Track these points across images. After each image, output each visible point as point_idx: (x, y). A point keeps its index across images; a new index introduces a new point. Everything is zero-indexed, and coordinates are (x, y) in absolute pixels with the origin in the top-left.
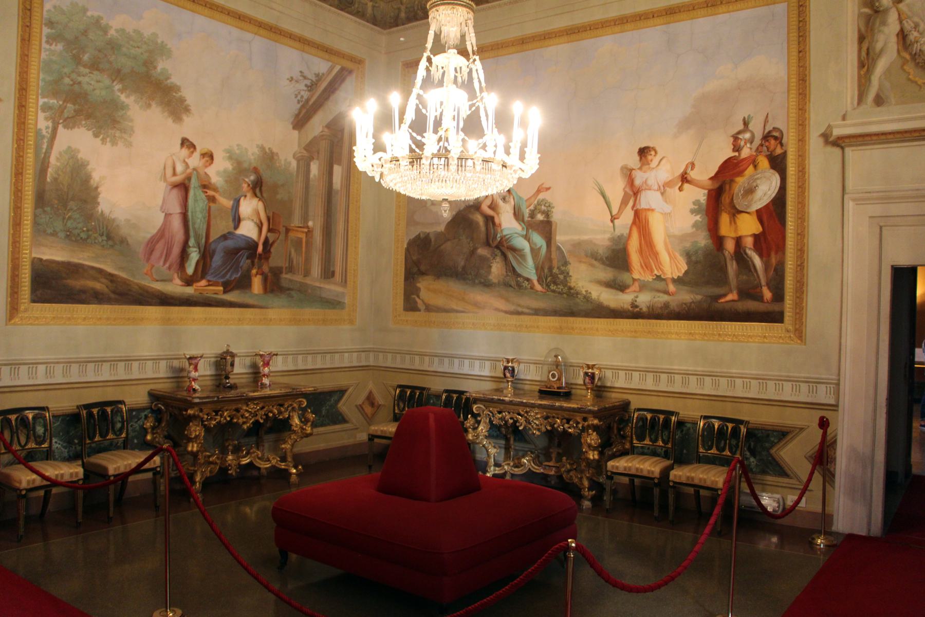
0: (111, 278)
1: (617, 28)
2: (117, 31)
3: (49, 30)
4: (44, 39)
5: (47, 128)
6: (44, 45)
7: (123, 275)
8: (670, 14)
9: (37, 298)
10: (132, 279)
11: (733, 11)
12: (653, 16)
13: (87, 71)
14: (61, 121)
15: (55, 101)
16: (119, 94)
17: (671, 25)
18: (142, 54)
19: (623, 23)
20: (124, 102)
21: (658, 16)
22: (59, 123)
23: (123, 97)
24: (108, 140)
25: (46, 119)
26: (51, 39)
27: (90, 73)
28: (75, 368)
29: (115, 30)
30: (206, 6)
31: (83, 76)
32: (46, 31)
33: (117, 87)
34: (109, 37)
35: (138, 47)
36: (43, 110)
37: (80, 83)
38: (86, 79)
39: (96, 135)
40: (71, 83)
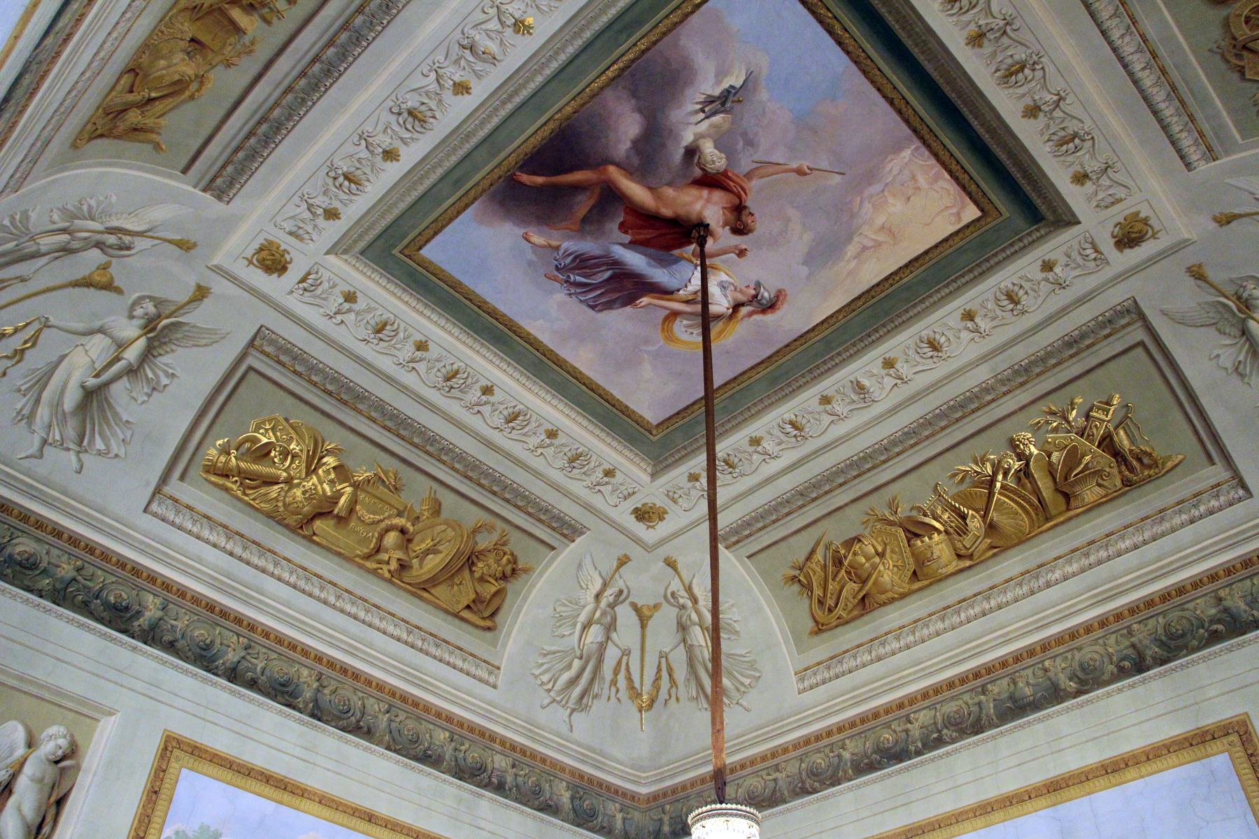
1: (980, 821)
8: (1055, 790)
11: (1149, 775)
12: (1030, 798)
17: (1059, 807)
19: (987, 813)
21: (1036, 797)
30: (386, 827)
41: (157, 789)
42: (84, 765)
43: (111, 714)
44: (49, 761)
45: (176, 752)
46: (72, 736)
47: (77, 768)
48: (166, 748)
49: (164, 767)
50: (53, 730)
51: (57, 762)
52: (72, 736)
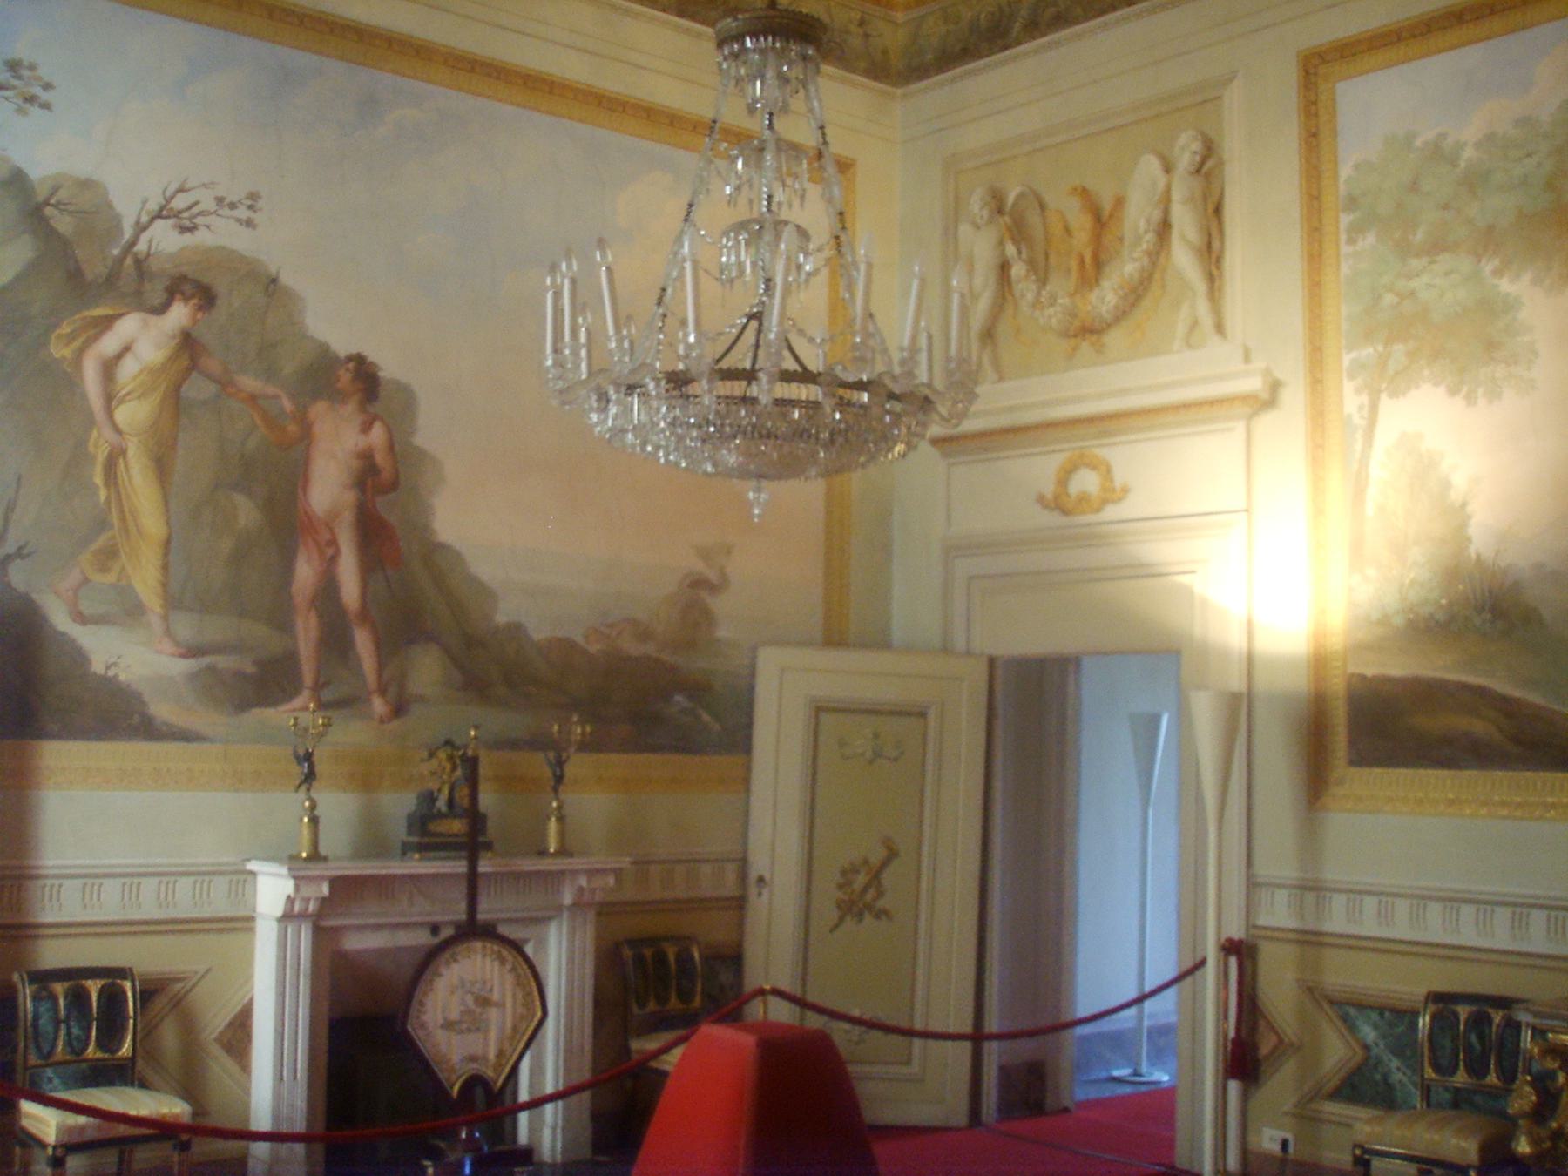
0: (1507, 707)
2: (1477, 145)
3: (1351, 217)
4: (1343, 237)
5: (1360, 408)
6: (1345, 249)
7: (1535, 698)
9: (1361, 759)
10: (1556, 707)
13: (1425, 260)
14: (1384, 386)
15: (1371, 350)
16: (1496, 281)
18: (1539, 165)
20: (1508, 294)
22: (1379, 391)
23: (1505, 285)
24: (1480, 391)
25: (1358, 391)
26: (1356, 231)
27: (1430, 263)
28: (1435, 909)
29: (1476, 144)
31: (1418, 276)
32: (1345, 219)
33: (1488, 267)
34: (1463, 164)
35: (1529, 155)
36: (1351, 377)
37: (1412, 293)
38: (1425, 279)
39: (1453, 392)
40: (1396, 300)
41: (1313, 130)
42: (1226, 156)
43: (1231, 80)
44: (1191, 173)
45: (1322, 70)
46: (1202, 134)
47: (1221, 163)
48: (1307, 72)
49: (1312, 98)
50: (1183, 138)
51: (1198, 171)
52: (1202, 134)
